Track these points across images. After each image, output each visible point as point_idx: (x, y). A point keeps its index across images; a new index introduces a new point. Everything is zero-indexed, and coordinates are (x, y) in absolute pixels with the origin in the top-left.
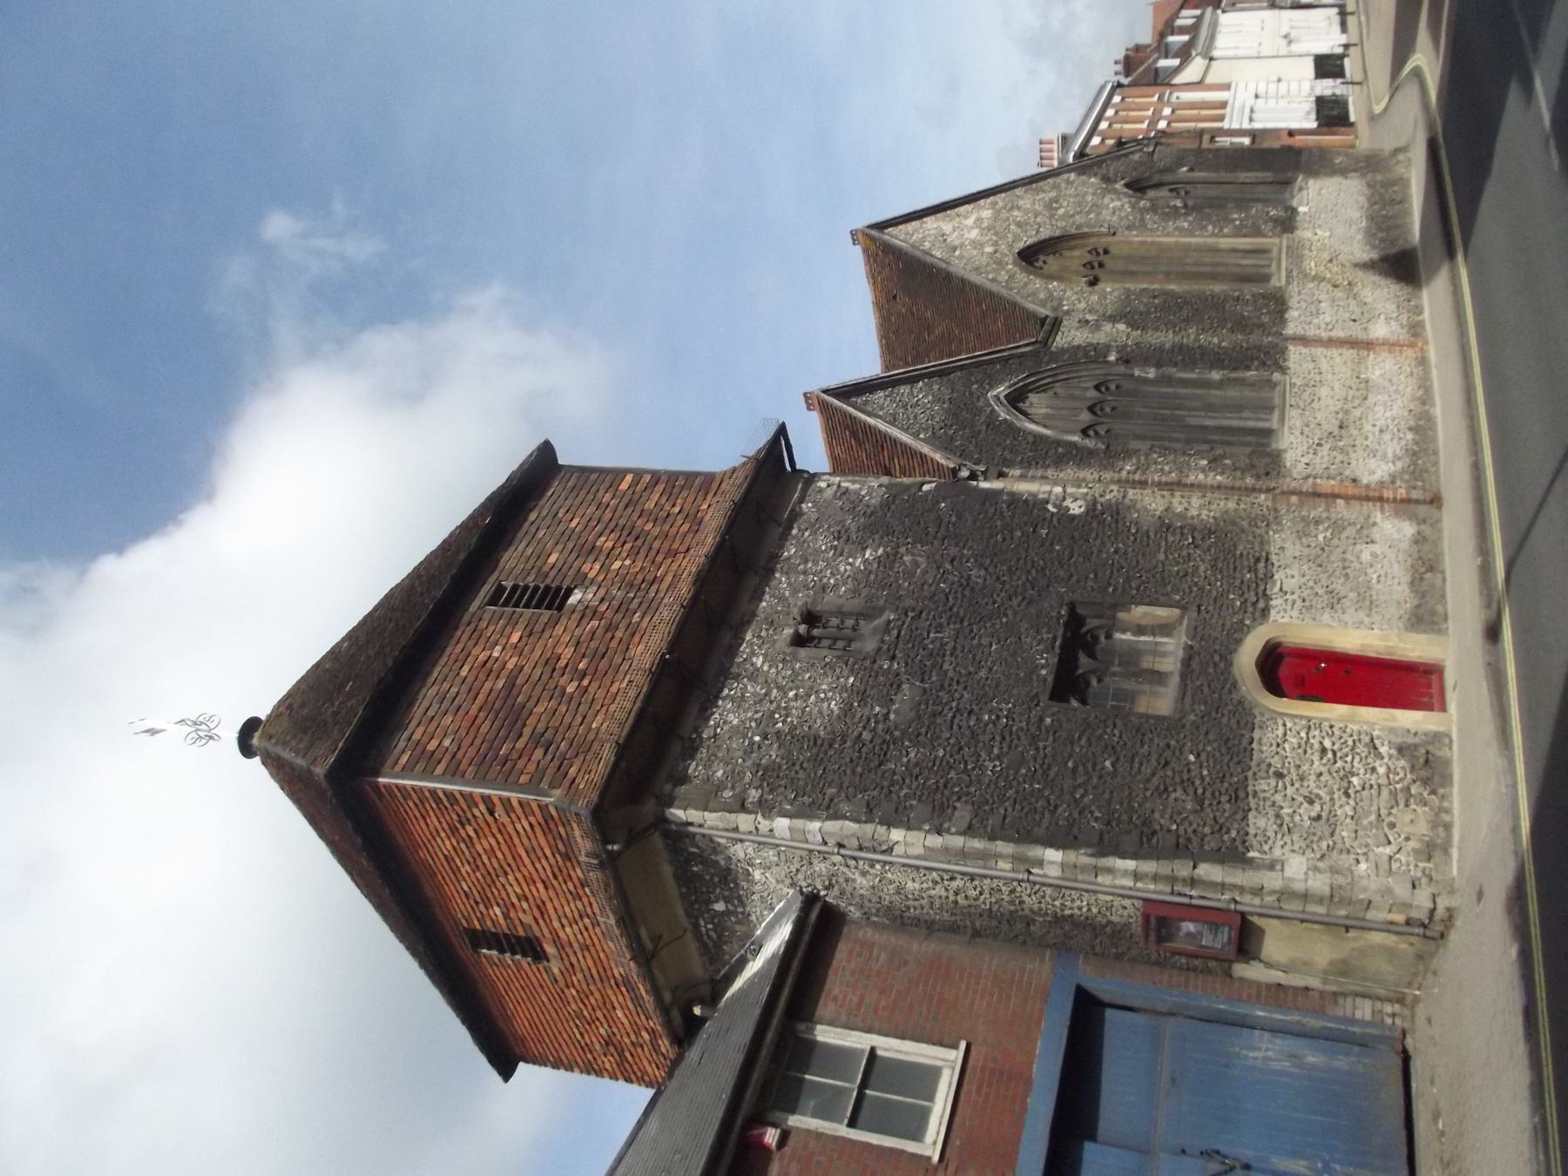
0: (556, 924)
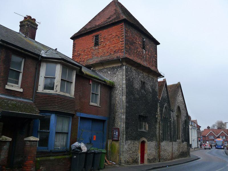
0: (102, 49)
